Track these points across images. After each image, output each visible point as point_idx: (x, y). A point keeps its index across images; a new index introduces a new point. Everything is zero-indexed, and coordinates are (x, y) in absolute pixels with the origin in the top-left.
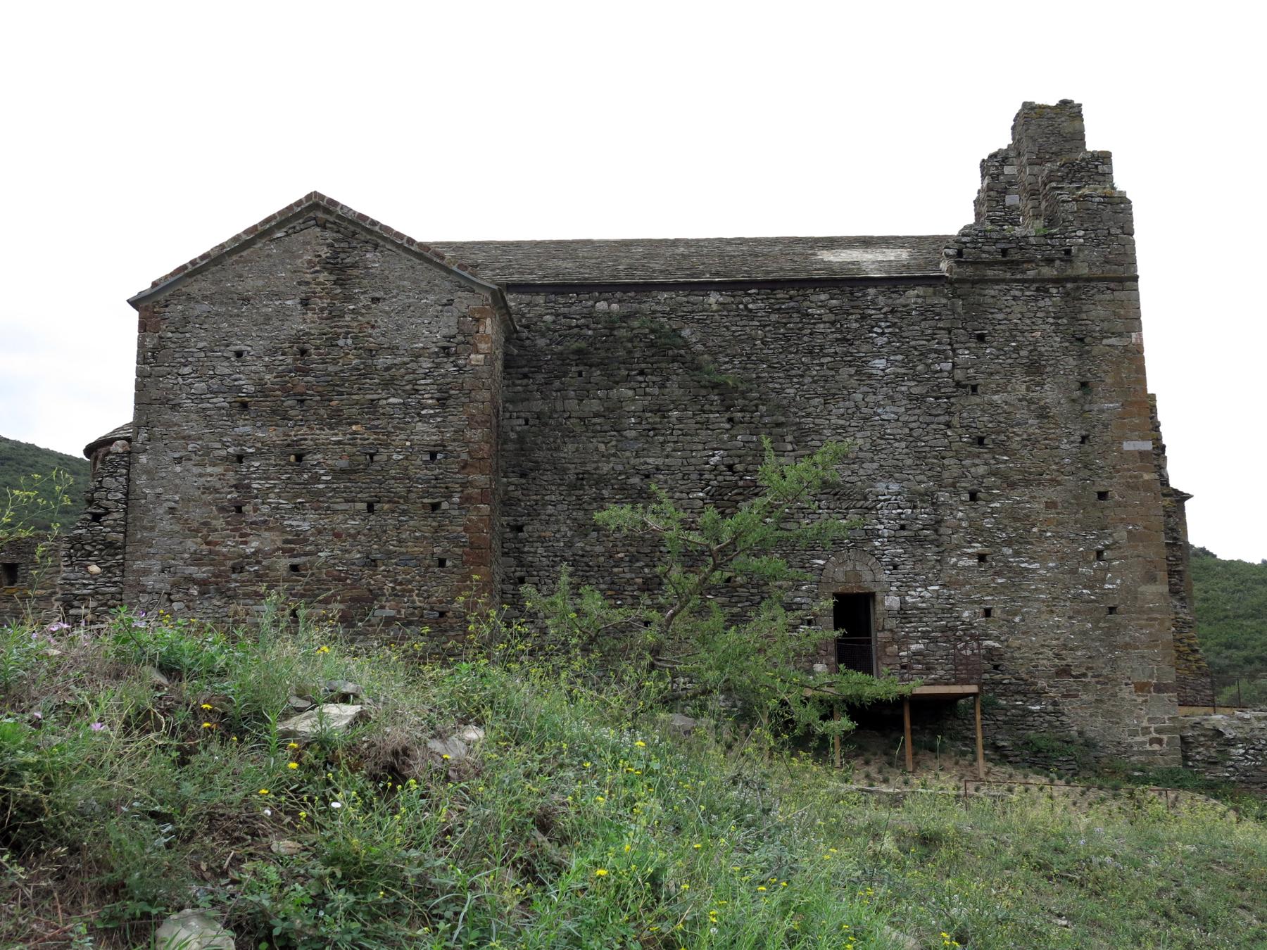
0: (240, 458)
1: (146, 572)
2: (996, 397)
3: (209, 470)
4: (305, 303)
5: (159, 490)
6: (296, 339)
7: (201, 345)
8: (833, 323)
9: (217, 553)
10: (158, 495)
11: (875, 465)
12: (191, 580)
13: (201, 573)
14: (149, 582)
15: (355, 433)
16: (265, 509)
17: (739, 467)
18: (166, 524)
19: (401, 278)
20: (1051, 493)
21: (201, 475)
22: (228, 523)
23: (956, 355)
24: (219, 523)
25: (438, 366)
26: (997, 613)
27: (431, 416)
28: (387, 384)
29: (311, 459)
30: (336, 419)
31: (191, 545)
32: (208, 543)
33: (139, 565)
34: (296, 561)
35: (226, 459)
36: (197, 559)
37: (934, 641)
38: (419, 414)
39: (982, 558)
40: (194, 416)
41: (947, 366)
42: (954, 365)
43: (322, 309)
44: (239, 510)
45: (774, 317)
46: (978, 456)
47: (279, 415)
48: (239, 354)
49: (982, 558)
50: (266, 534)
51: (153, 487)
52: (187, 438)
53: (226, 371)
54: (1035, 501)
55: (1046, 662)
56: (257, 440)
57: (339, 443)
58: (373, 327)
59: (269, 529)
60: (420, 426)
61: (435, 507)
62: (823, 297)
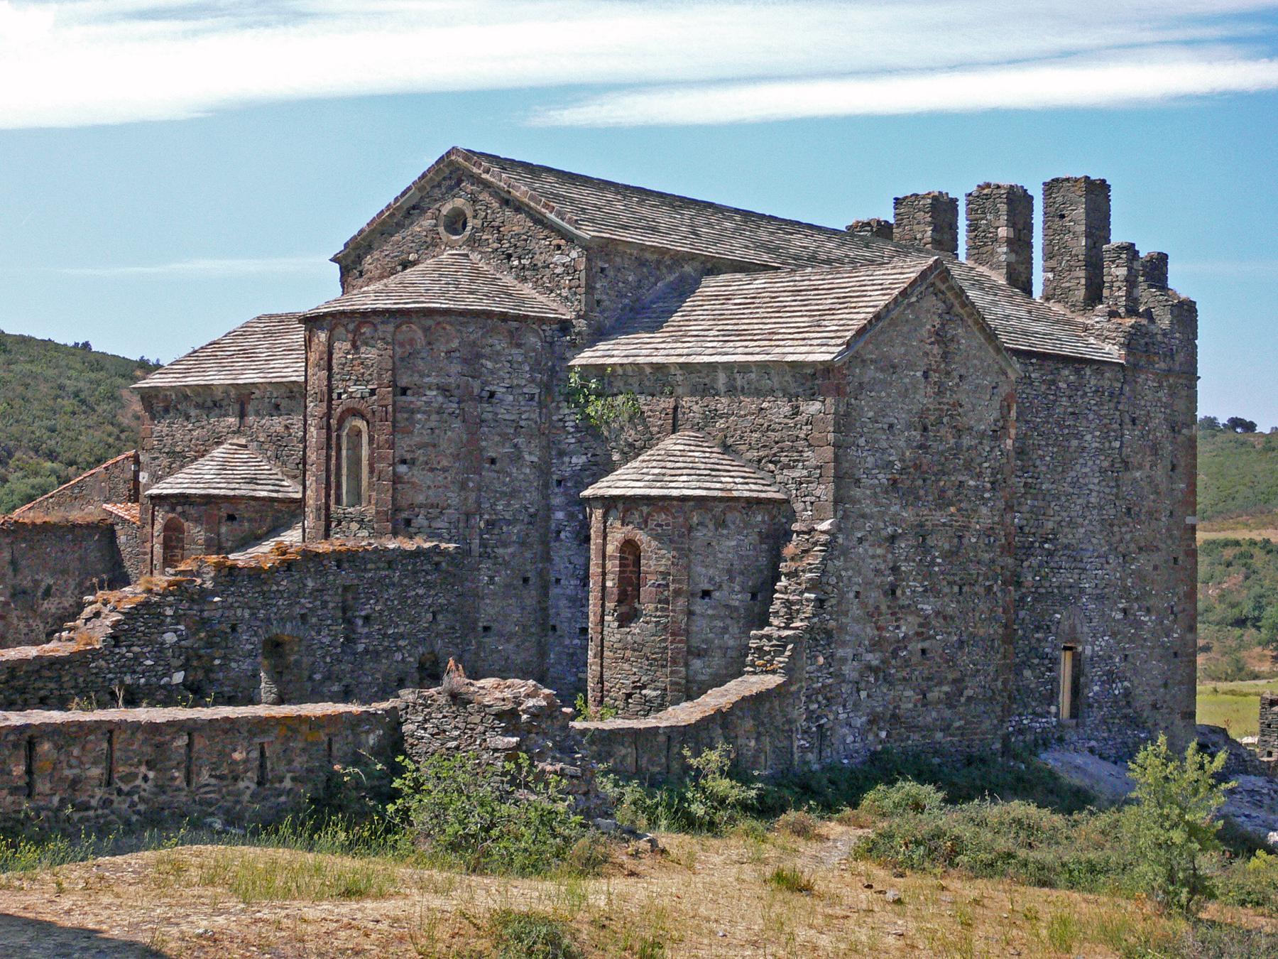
0: (893, 538)
1: (843, 660)
2: (1138, 474)
3: (879, 551)
4: (926, 375)
5: (850, 573)
6: (923, 414)
7: (871, 414)
8: (1070, 397)
9: (885, 639)
10: (850, 578)
11: (1083, 530)
12: (870, 668)
13: (873, 659)
14: (846, 670)
15: (952, 515)
16: (908, 592)
17: (1026, 530)
18: (856, 610)
19: (975, 357)
20: (1157, 558)
21: (873, 557)
22: (889, 607)
23: (1122, 436)
24: (883, 608)
25: (992, 449)
26: (1130, 658)
27: (989, 499)
28: (968, 466)
29: (931, 541)
30: (942, 502)
31: (870, 631)
32: (878, 629)
33: (840, 653)
34: (926, 645)
35: (887, 539)
36: (876, 645)
37: (1103, 682)
38: (983, 498)
39: (1125, 611)
40: (868, 492)
41: (1117, 444)
42: (1122, 443)
43: (935, 383)
44: (894, 592)
45: (1044, 388)
46: (1126, 524)
47: (911, 497)
48: (891, 426)
49: (1125, 611)
50: (910, 619)
51: (846, 570)
52: (864, 516)
53: (885, 445)
54: (1142, 562)
55: (1149, 699)
56: (903, 520)
57: (944, 524)
58: (961, 406)
59: (912, 612)
60: (984, 510)
61: (990, 587)
62: (1067, 372)
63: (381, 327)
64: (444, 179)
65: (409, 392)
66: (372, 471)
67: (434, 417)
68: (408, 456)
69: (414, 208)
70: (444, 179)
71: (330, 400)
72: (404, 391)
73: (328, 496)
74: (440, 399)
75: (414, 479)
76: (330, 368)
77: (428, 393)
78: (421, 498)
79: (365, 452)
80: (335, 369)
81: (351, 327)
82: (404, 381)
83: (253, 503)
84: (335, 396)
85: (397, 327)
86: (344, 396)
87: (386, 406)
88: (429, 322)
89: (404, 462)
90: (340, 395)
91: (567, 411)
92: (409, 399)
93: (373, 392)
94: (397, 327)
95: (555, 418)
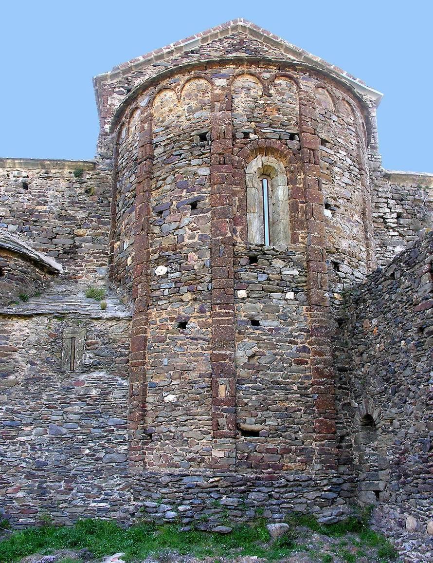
63: (303, 83)
64: (226, 38)
65: (328, 145)
66: (294, 208)
67: (347, 174)
68: (332, 202)
69: (192, 52)
70: (226, 38)
71: (234, 138)
72: (324, 142)
73: (234, 231)
74: (349, 161)
75: (338, 225)
76: (230, 108)
77: (340, 151)
78: (344, 244)
79: (282, 192)
80: (240, 111)
81: (267, 75)
82: (323, 136)
83: (21, 262)
84: (239, 135)
85: (317, 87)
86: (252, 136)
87: (313, 150)
88: (338, 93)
89: (327, 206)
90: (246, 135)
91: (388, 210)
92: (329, 151)
93: (292, 137)
94: (317, 87)
95: (376, 215)
